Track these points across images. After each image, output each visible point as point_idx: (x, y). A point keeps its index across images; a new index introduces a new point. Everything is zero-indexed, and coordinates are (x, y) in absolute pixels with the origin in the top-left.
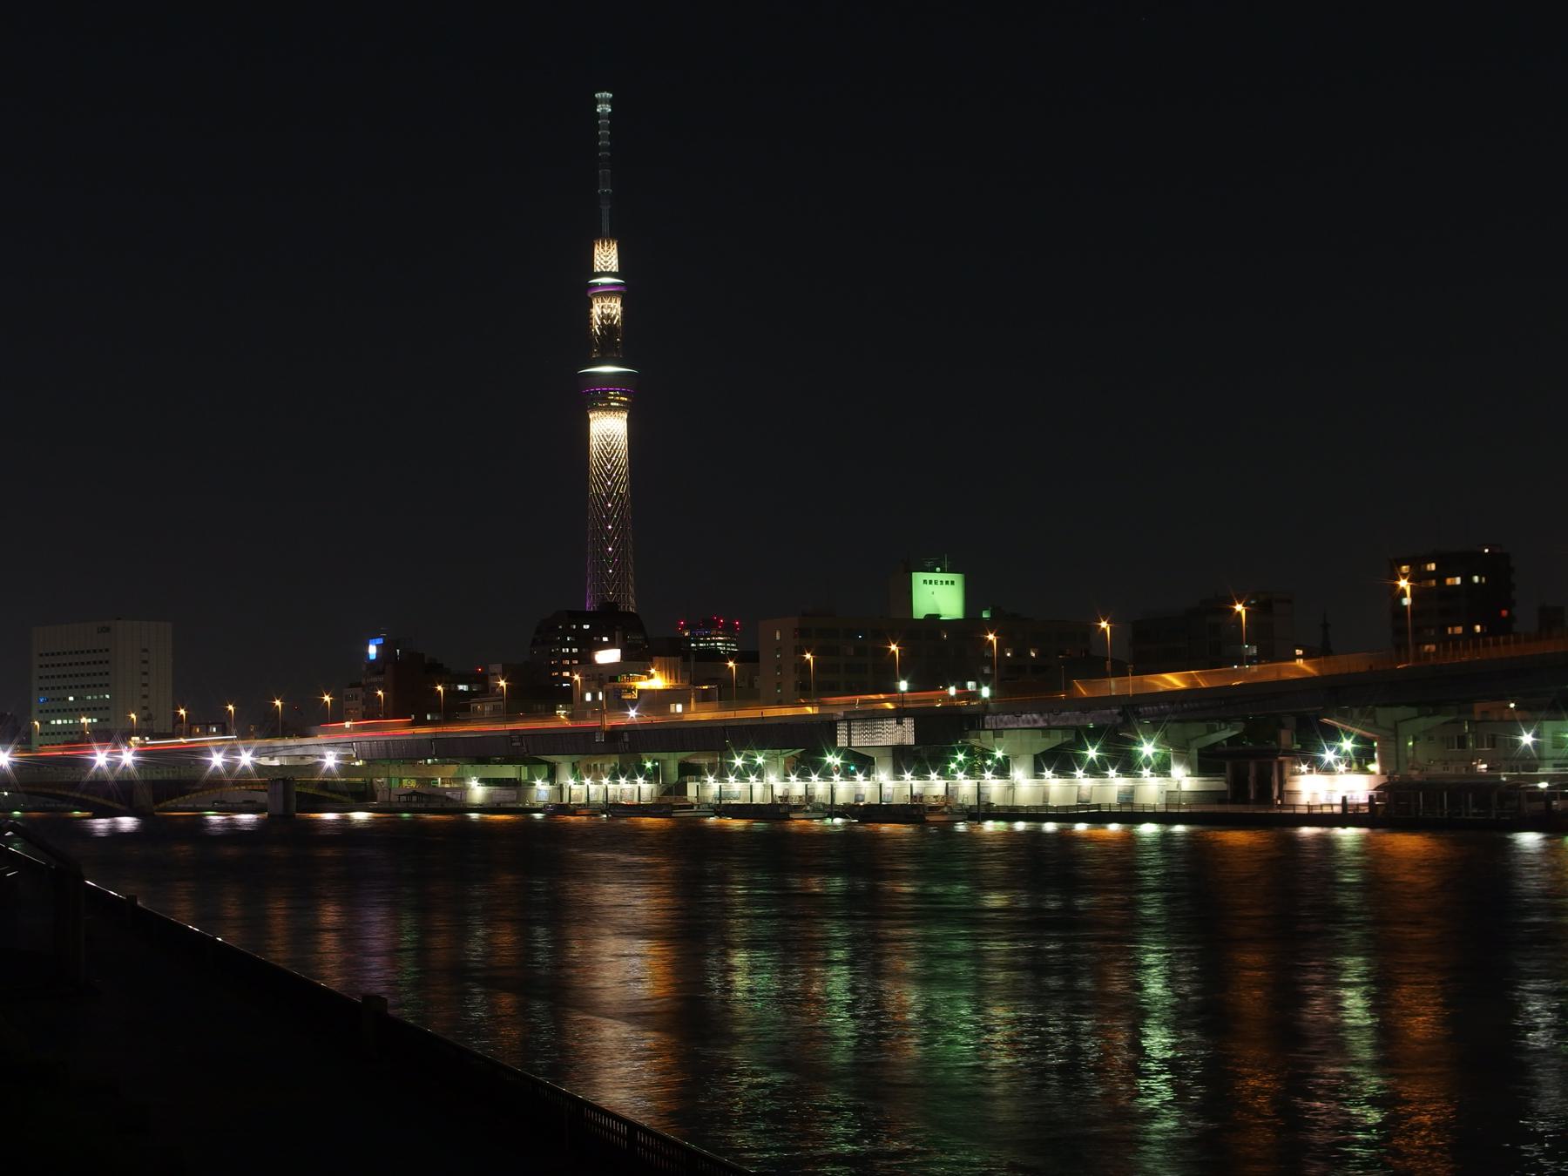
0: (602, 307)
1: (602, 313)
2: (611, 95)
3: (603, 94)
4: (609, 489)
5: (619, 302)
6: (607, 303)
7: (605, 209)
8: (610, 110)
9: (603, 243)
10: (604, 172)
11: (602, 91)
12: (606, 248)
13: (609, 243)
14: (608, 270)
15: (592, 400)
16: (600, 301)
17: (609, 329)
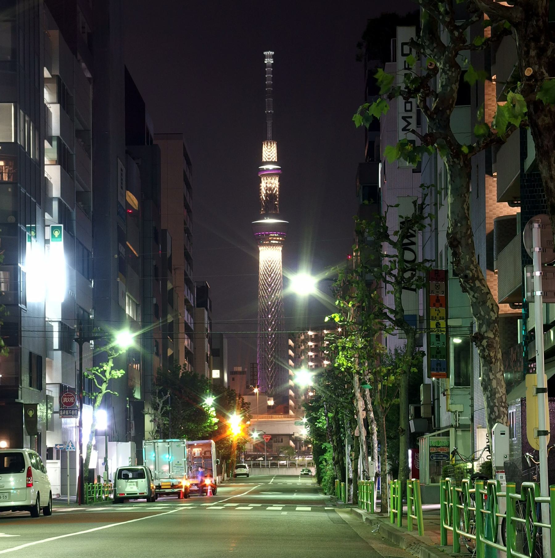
0: (266, 183)
1: (266, 186)
2: (273, 53)
3: (268, 53)
4: (270, 293)
5: (277, 179)
6: (269, 180)
7: (269, 123)
8: (273, 62)
9: (267, 144)
10: (269, 100)
11: (268, 51)
12: (269, 147)
13: (271, 144)
14: (270, 160)
15: (260, 239)
16: (265, 178)
17: (271, 196)
